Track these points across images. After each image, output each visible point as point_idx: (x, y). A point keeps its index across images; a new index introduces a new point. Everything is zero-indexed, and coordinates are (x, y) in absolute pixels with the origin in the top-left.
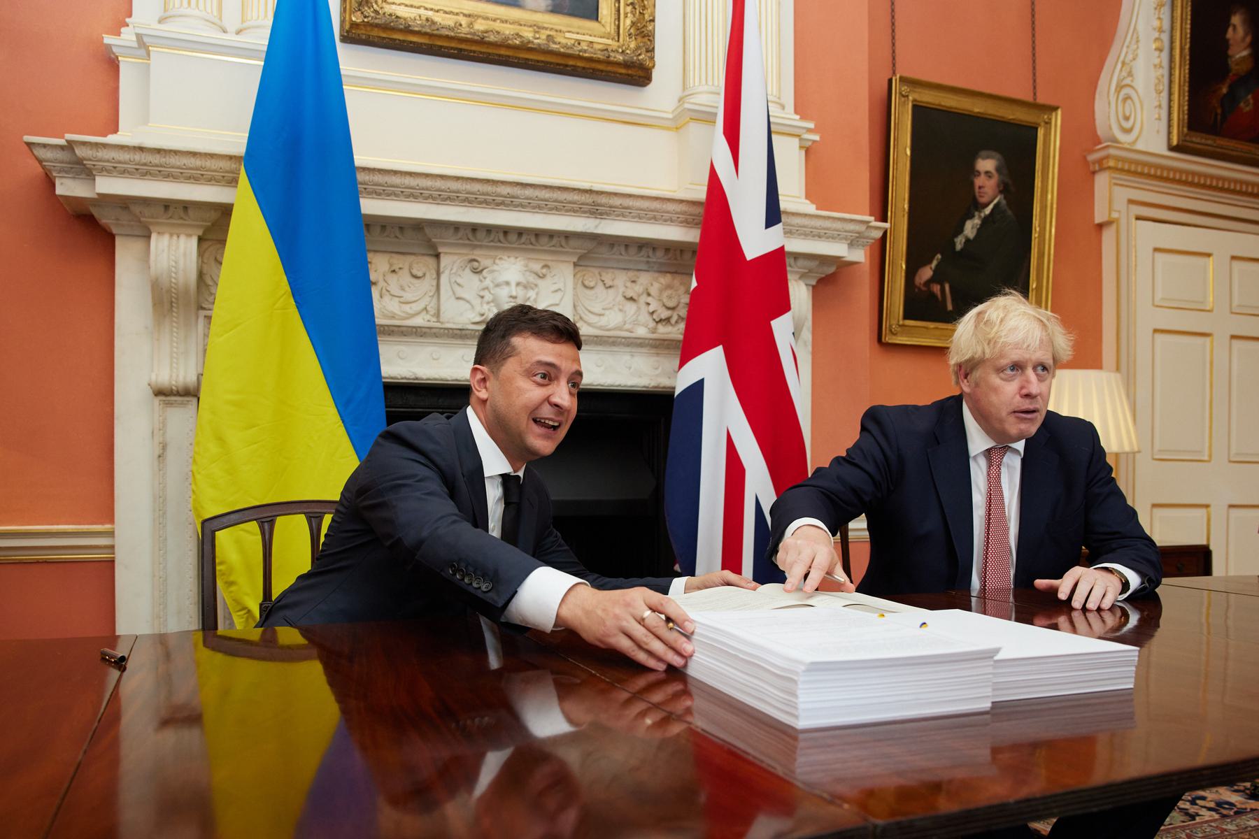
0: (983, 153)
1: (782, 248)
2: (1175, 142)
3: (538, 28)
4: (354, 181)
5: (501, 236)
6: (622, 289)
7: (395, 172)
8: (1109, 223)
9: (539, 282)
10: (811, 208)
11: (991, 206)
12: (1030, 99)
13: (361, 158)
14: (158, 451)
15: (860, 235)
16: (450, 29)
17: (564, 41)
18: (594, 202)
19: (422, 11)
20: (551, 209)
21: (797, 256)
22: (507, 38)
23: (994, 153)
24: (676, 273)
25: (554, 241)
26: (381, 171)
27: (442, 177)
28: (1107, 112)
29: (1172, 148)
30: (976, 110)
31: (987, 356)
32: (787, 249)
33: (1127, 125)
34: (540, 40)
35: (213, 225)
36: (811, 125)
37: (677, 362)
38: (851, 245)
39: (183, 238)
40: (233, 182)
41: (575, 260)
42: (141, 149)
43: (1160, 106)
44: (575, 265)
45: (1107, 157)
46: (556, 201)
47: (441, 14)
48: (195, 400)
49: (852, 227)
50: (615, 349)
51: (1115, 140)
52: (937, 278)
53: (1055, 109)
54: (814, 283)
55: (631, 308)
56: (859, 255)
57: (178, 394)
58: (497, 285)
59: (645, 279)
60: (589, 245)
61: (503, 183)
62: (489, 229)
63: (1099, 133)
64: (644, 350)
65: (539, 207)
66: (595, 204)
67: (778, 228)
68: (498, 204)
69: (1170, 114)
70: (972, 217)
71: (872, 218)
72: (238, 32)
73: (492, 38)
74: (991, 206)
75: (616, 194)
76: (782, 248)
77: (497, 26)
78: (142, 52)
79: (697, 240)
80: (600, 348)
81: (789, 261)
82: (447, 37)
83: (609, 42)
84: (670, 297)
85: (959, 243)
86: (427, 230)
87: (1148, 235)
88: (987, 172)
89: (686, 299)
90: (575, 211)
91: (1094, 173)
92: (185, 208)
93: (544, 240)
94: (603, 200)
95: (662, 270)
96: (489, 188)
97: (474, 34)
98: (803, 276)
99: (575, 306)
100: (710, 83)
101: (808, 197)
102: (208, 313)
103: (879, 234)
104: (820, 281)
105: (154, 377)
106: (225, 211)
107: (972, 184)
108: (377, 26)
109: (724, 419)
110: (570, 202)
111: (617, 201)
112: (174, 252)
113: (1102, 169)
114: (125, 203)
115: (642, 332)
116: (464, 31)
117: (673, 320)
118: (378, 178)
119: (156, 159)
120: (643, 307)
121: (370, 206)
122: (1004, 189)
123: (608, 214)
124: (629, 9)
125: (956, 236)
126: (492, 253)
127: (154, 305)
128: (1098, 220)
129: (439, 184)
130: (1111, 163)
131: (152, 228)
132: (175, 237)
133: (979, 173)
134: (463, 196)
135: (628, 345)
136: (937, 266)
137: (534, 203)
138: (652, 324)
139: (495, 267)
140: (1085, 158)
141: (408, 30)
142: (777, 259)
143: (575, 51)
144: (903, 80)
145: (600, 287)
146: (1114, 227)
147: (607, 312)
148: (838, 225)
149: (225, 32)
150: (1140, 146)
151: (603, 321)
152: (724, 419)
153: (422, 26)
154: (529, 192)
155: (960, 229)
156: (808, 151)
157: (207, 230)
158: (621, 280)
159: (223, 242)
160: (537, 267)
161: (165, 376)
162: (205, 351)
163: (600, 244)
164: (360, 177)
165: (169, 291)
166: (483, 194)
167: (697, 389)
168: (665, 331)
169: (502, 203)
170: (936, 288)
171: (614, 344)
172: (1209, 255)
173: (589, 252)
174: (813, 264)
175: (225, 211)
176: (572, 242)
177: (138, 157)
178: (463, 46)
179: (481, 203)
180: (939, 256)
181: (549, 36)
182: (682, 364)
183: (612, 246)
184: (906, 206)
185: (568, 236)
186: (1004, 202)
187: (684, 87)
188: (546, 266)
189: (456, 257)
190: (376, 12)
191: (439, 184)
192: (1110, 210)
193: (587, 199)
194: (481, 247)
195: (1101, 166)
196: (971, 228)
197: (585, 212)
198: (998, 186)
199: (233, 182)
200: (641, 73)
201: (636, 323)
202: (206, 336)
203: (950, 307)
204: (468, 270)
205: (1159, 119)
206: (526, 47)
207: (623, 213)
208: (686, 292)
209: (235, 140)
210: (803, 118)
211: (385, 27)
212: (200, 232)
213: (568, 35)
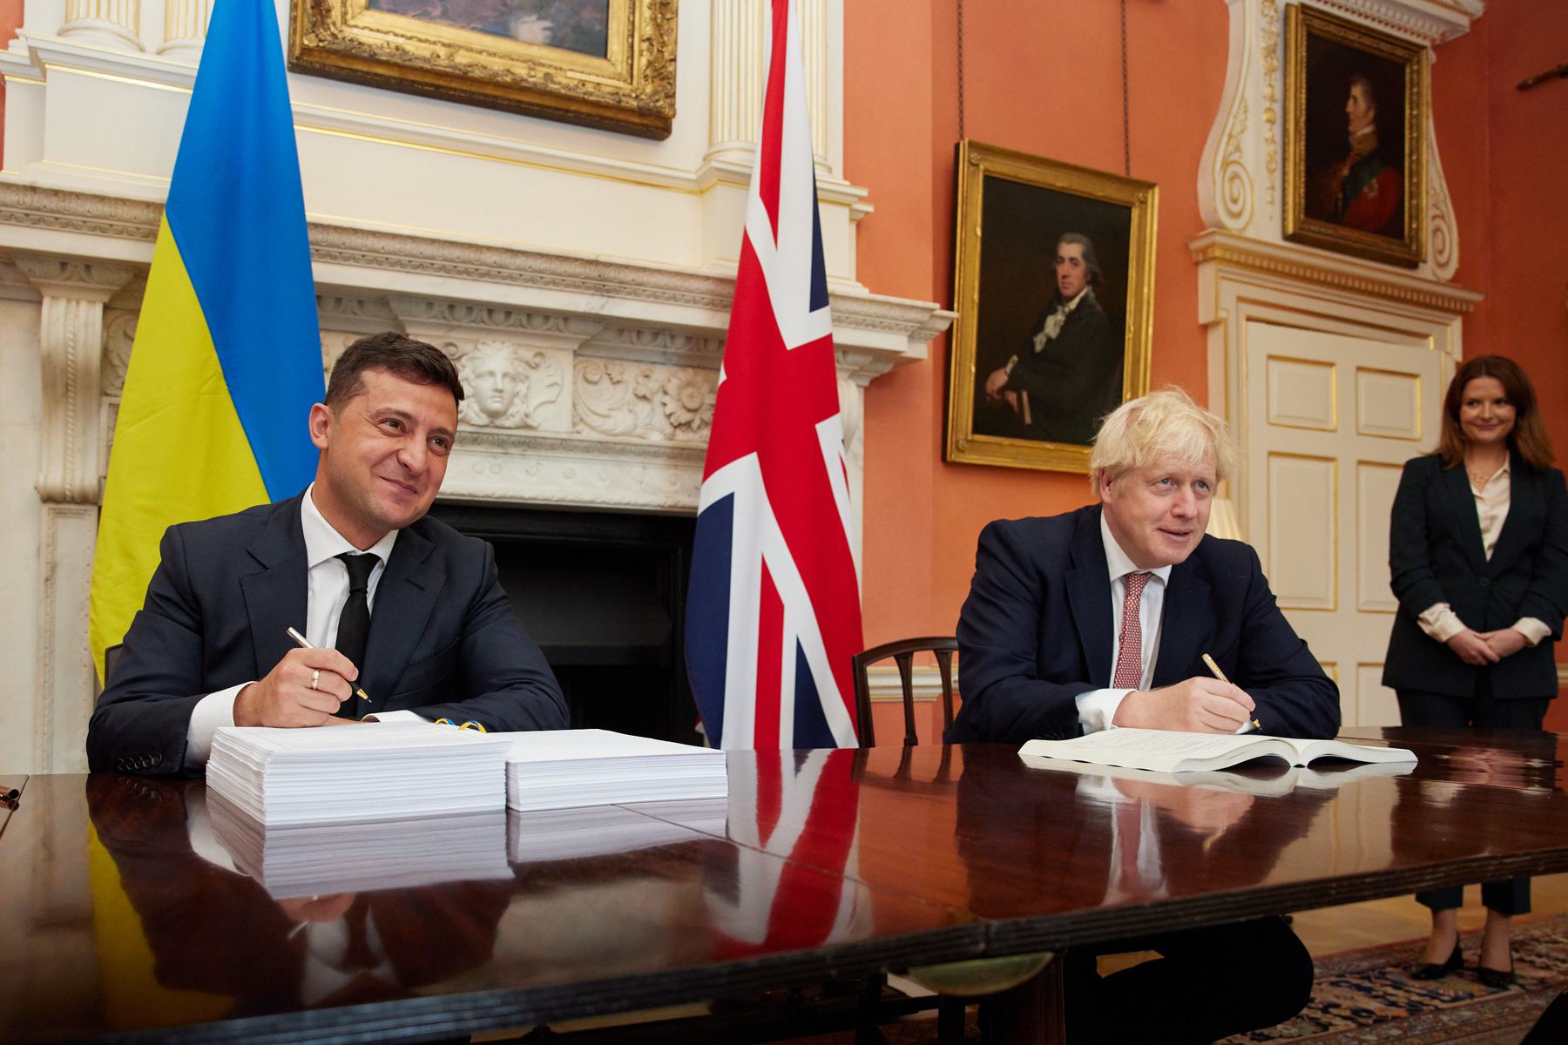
0: (1068, 236)
1: (829, 337)
2: (1290, 230)
3: (533, 64)
4: (305, 242)
5: (485, 316)
6: (632, 385)
7: (355, 231)
8: (1215, 324)
9: (532, 373)
10: (864, 292)
11: (1077, 300)
12: (1122, 174)
13: (314, 213)
14: (45, 573)
15: (922, 326)
16: (425, 60)
17: (564, 81)
18: (600, 275)
19: (391, 38)
20: (547, 283)
21: (847, 350)
22: (497, 74)
23: (1079, 236)
24: (699, 367)
25: (551, 323)
26: (337, 229)
27: (414, 239)
28: (1211, 192)
29: (1287, 238)
30: (1059, 184)
31: (1138, 464)
32: (836, 340)
33: (1236, 208)
34: (537, 77)
35: (124, 290)
36: (864, 193)
37: (701, 477)
38: (912, 338)
39: (83, 305)
40: (151, 236)
41: (576, 347)
42: (33, 189)
43: (1272, 188)
44: (576, 354)
45: (1213, 245)
46: (553, 273)
47: (414, 42)
48: (94, 510)
49: (912, 315)
50: (622, 458)
51: (1222, 226)
52: (1014, 384)
53: (1151, 186)
54: (866, 383)
55: (643, 408)
56: (921, 351)
57: (73, 501)
58: (479, 376)
59: (661, 374)
60: (593, 329)
61: (489, 248)
62: (470, 306)
63: (1203, 216)
64: (659, 461)
65: (533, 280)
66: (601, 278)
67: (824, 312)
68: (483, 275)
69: (1284, 196)
70: (1053, 311)
71: (937, 306)
72: (160, 52)
73: (477, 73)
75: (627, 267)
76: (829, 337)
77: (483, 59)
78: (36, 71)
79: (726, 326)
80: (605, 457)
81: (838, 355)
82: (422, 70)
83: (621, 84)
84: (691, 396)
85: (1039, 342)
86: (394, 305)
87: (1260, 340)
88: (1072, 259)
89: (711, 399)
90: (576, 287)
91: (1197, 264)
92: (88, 267)
93: (537, 321)
94: (611, 273)
95: (686, 362)
96: (471, 255)
97: (455, 67)
98: (853, 375)
99: (574, 405)
100: (743, 137)
101: (859, 279)
102: (114, 400)
103: (944, 326)
104: (874, 382)
105: (42, 479)
106: (139, 272)
107: (1055, 272)
108: (335, 52)
109: (759, 544)
110: (571, 276)
111: (628, 276)
112: (73, 322)
113: (1205, 261)
115: (656, 438)
116: (443, 63)
117: (695, 425)
118: (334, 238)
119: (52, 203)
120: (659, 408)
121: (324, 272)
122: (1092, 280)
123: (617, 291)
124: (645, 45)
126: (472, 336)
127: (45, 388)
128: (1202, 320)
129: (409, 247)
130: (1218, 253)
131: (44, 291)
132: (73, 304)
133: (1062, 260)
134: (439, 263)
135: (640, 454)
136: (1013, 371)
137: (527, 275)
138: (669, 430)
139: (477, 354)
140: (1187, 246)
141: (372, 59)
142: (823, 350)
143: (579, 93)
144: (973, 146)
145: (606, 383)
146: (1221, 328)
147: (614, 413)
148: (897, 313)
149: (142, 50)
150: (1250, 234)
151: (609, 425)
152: (759, 544)
153: (390, 55)
154: (520, 261)
155: (1040, 327)
156: (859, 225)
157: (115, 297)
158: (631, 373)
159: (136, 313)
160: (528, 354)
161: (57, 478)
162: (109, 447)
163: (606, 328)
164: (313, 235)
165: (65, 371)
166: (464, 262)
167: (725, 507)
168: (683, 437)
169: (487, 274)
170: (1012, 397)
171: (622, 452)
172: (1331, 365)
173: (593, 338)
175: (139, 272)
176: (573, 325)
177: (28, 199)
178: (441, 82)
179: (460, 273)
180: (1015, 358)
181: (547, 74)
182: (707, 475)
183: (621, 331)
184: (976, 297)
185: (567, 317)
186: (1092, 295)
187: (711, 143)
188: (539, 354)
190: (333, 35)
191: (409, 247)
192: (1217, 308)
193: (593, 271)
194: (459, 327)
195: (1206, 256)
196: (1053, 325)
197: (589, 288)
198: (1085, 276)
199: (151, 236)
200: (658, 123)
201: (650, 427)
202: (112, 429)
203: (1028, 420)
205: (1272, 202)
206: (518, 86)
207: (635, 290)
208: (711, 391)
209: (156, 184)
210: (854, 183)
211: (346, 55)
212: (106, 299)
213: (570, 74)
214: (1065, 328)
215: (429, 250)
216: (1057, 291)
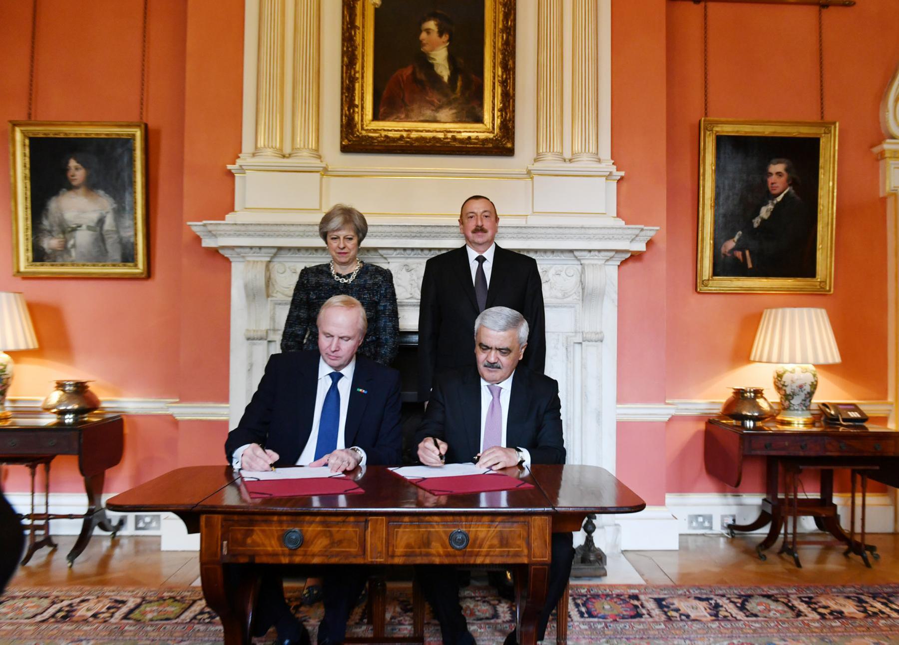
0: (774, 161)
11: (782, 195)
23: (783, 160)
70: (766, 204)
74: (782, 195)
85: (756, 222)
96: (407, 229)
104: (624, 262)
114: (232, 248)
119: (243, 228)
122: (792, 182)
125: (754, 218)
133: (771, 174)
136: (738, 240)
137: (433, 235)
154: (429, 229)
155: (757, 213)
174: (612, 254)
180: (740, 233)
186: (793, 191)
196: (765, 212)
198: (788, 181)
204: (404, 270)
214: (774, 213)
216: (768, 192)
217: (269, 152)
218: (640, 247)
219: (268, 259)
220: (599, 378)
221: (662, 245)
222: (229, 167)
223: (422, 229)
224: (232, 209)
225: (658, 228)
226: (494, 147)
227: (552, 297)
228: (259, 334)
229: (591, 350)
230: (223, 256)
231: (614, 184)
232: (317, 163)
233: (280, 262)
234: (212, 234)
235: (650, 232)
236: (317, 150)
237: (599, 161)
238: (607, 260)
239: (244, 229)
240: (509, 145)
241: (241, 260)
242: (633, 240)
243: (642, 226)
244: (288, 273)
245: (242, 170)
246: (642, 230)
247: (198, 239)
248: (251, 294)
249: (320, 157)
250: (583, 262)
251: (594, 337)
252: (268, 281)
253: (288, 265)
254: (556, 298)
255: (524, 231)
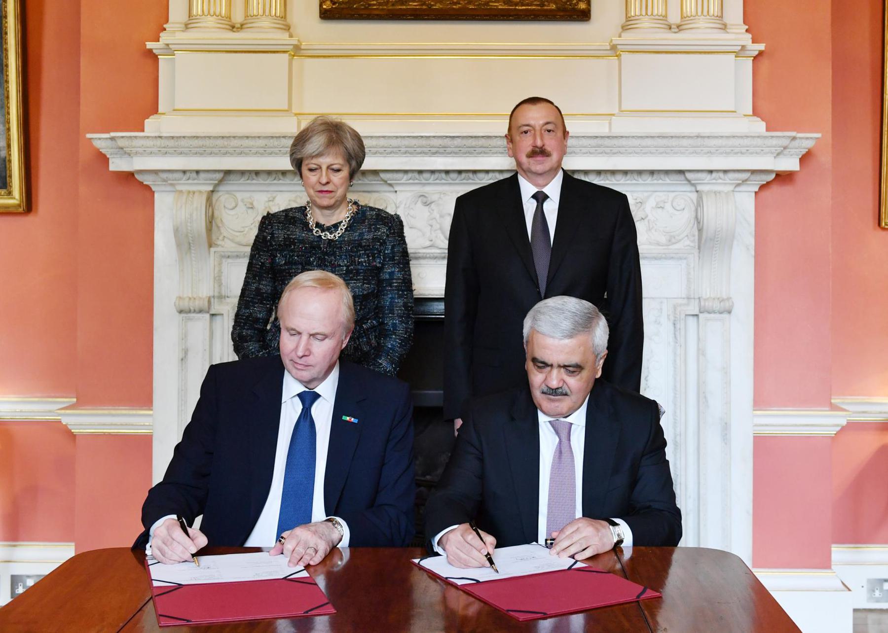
96: (424, 142)
104: (762, 187)
114: (156, 172)
134: (403, 150)
137: (464, 150)
154: (457, 142)
189: (409, 194)
204: (419, 204)
215: (395, 142)
217: (211, 21)
218: (791, 164)
219: (211, 188)
220: (726, 371)
221: (825, 158)
222: (150, 45)
223: (447, 142)
224: (154, 110)
225: (819, 135)
226: (558, 9)
227: (650, 244)
228: (197, 304)
229: (713, 326)
230: (141, 183)
231: (749, 63)
232: (282, 38)
233: (228, 192)
234: (123, 152)
235: (807, 140)
236: (284, 17)
237: (724, 27)
238: (738, 185)
239: (173, 144)
240: (582, 6)
241: (169, 188)
242: (778, 154)
243: (793, 134)
244: (242, 207)
245: (169, 50)
246: (794, 138)
247: (103, 159)
248: (185, 243)
249: (288, 28)
250: (699, 188)
251: (717, 306)
252: (211, 222)
253: (239, 196)
254: (658, 244)
255: (607, 142)
